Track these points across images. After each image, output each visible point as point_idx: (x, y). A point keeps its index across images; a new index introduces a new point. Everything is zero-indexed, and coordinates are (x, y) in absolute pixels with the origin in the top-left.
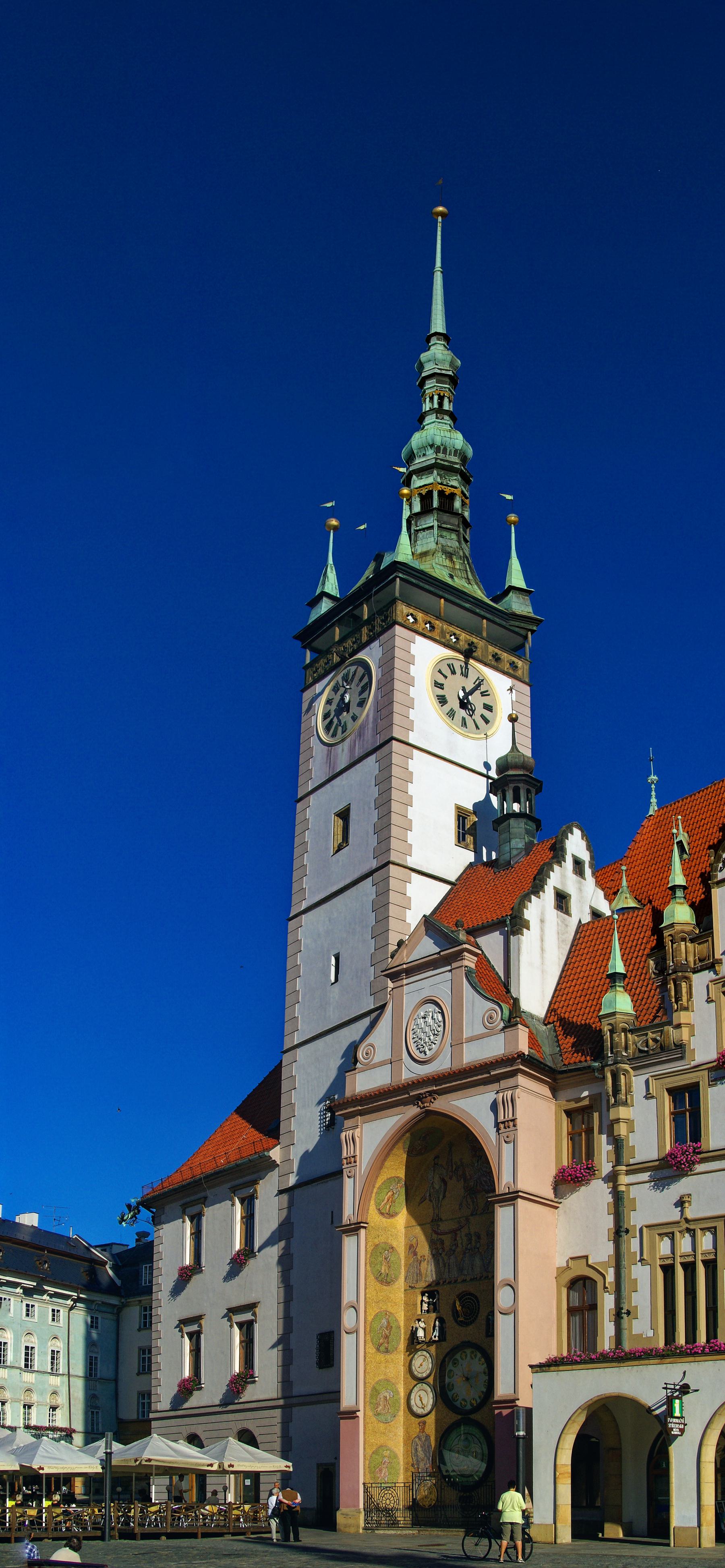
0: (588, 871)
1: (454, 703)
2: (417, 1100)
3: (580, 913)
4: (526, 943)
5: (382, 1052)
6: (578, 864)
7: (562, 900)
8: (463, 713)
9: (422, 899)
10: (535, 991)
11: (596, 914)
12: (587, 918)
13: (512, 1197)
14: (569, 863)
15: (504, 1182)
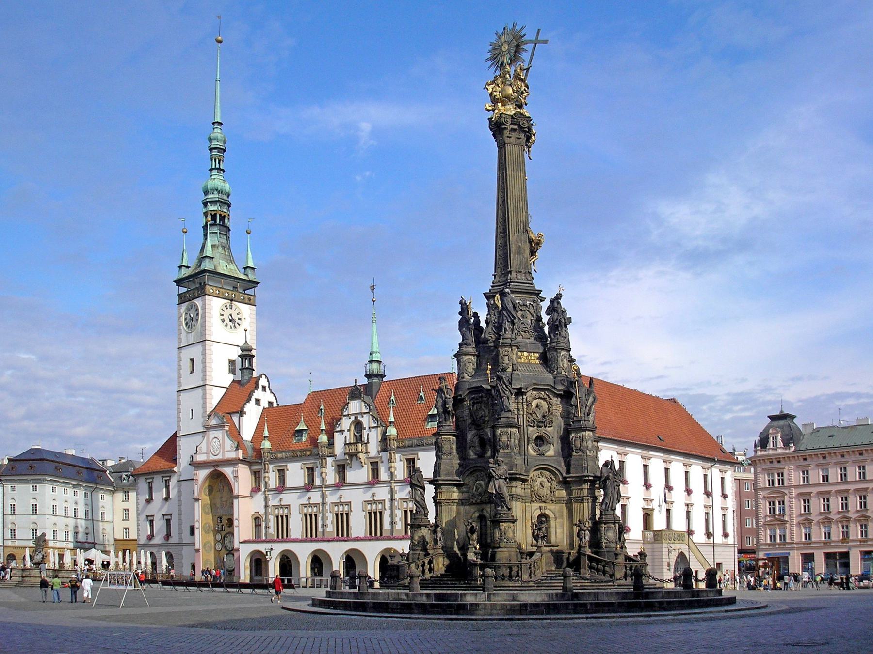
0: (267, 389)
1: (227, 321)
2: (214, 466)
3: (264, 404)
4: (244, 419)
5: (204, 450)
6: (264, 388)
7: (258, 402)
8: (231, 323)
9: (215, 396)
10: (247, 434)
11: (270, 403)
12: (267, 406)
13: (237, 497)
14: (260, 387)
15: (235, 493)
